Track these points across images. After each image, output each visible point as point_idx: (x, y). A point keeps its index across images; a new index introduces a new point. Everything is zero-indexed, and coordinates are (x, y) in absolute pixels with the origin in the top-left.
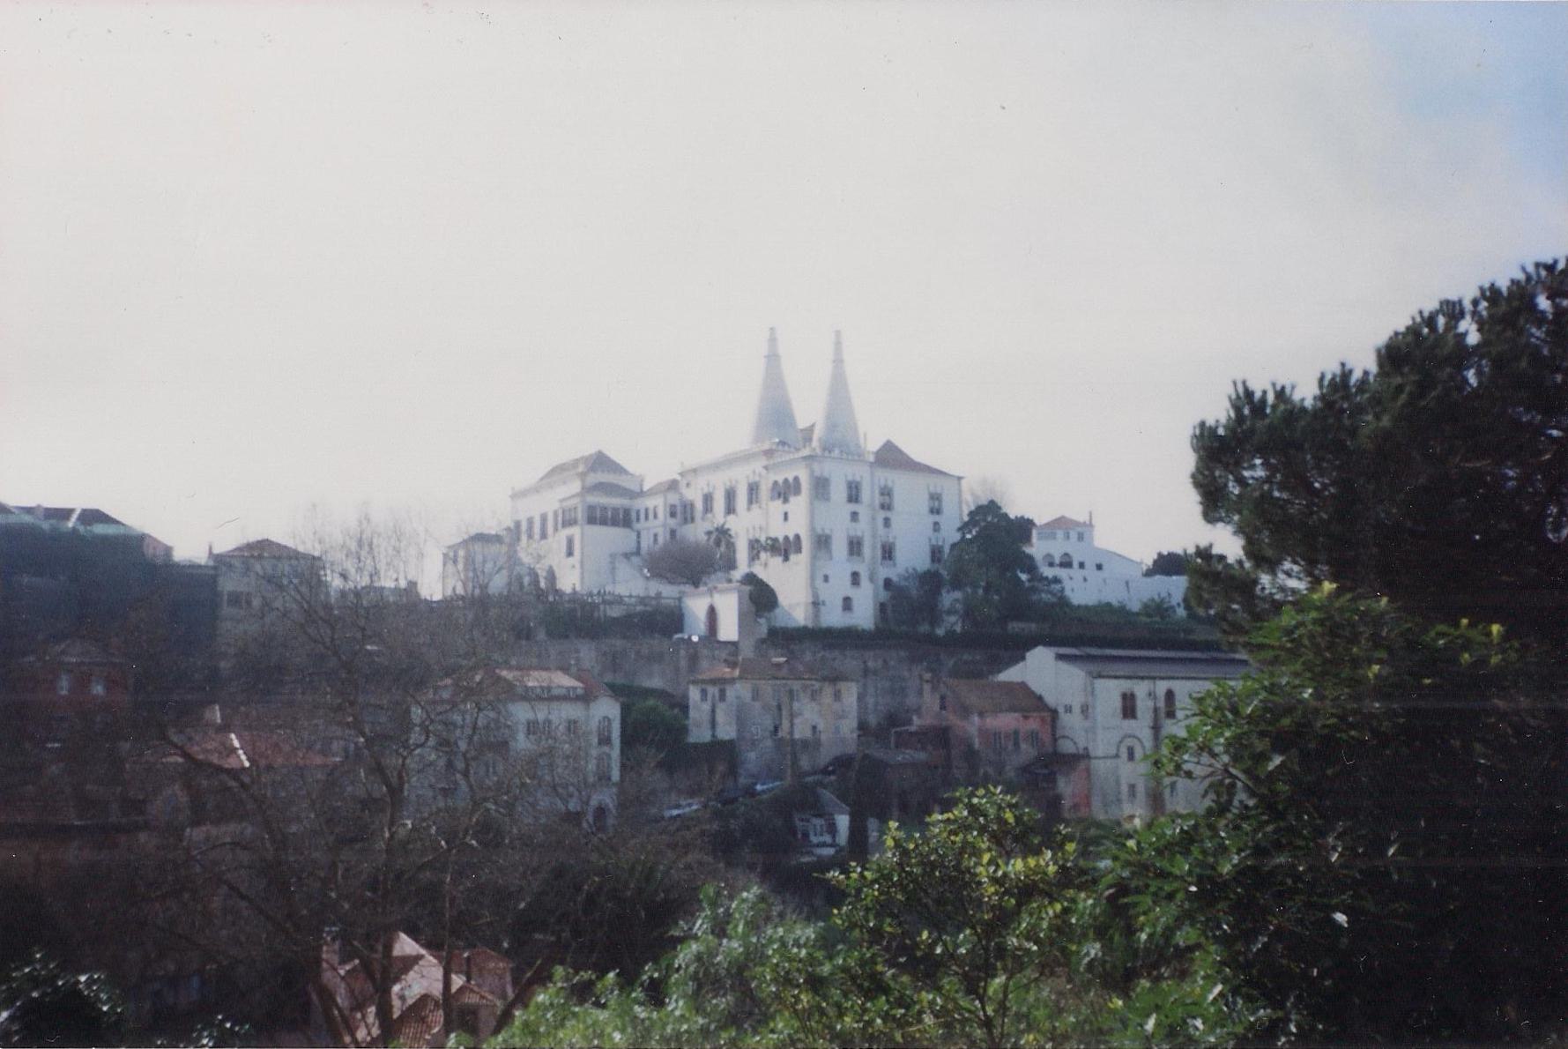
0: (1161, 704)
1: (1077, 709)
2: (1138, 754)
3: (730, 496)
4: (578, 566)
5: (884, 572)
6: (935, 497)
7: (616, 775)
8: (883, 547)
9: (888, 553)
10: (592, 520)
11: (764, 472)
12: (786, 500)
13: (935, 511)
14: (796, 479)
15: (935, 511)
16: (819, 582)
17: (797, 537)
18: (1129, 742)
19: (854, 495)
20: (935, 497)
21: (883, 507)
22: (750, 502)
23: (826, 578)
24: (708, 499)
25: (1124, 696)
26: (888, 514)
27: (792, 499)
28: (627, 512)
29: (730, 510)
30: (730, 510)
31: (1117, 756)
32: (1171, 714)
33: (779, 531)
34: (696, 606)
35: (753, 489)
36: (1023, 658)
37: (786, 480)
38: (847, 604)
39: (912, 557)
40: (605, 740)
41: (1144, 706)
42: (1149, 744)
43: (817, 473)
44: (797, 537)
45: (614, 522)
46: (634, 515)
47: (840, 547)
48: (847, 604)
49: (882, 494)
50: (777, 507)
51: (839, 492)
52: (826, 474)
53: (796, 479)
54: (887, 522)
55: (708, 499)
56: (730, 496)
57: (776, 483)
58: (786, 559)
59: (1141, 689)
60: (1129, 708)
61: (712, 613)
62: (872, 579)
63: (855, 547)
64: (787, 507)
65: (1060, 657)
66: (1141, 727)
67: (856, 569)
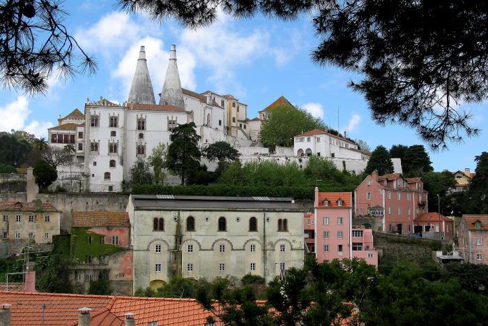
0: (184, 224)
2: (164, 248)
19: (114, 122)
23: (95, 164)
31: (148, 250)
38: (107, 176)
41: (170, 225)
43: (92, 113)
47: (104, 148)
48: (107, 176)
51: (104, 121)
52: (97, 114)
54: (141, 136)
59: (169, 217)
60: (159, 225)
62: (122, 163)
63: (113, 148)
66: (168, 235)
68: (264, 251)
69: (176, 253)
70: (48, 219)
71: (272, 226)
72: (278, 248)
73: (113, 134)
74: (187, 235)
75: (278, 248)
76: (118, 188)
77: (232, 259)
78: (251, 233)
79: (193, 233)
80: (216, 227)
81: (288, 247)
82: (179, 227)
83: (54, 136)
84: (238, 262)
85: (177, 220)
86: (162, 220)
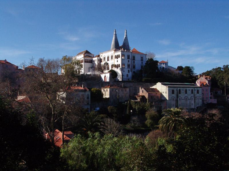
1: (165, 92)
2: (175, 99)
3: (108, 58)
4: (83, 69)
5: (133, 70)
6: (142, 58)
7: (90, 104)
8: (133, 66)
9: (134, 67)
10: (85, 62)
11: (113, 54)
12: (117, 59)
13: (142, 60)
14: (119, 55)
15: (142, 60)
16: (123, 72)
17: (119, 64)
18: (173, 98)
20: (142, 58)
21: (133, 59)
22: (111, 59)
24: (104, 58)
25: (172, 90)
26: (134, 61)
27: (118, 58)
28: (91, 60)
29: (108, 60)
30: (108, 60)
31: (171, 100)
32: (180, 93)
33: (116, 63)
34: (103, 76)
35: (112, 57)
36: (156, 84)
37: (117, 55)
39: (138, 67)
40: (88, 98)
41: (175, 92)
42: (176, 98)
44: (119, 64)
45: (89, 62)
46: (92, 61)
49: (133, 57)
50: (116, 60)
52: (124, 54)
53: (119, 55)
54: (134, 62)
55: (104, 58)
56: (108, 58)
57: (116, 56)
58: (117, 68)
61: (105, 76)
62: (131, 71)
63: (129, 66)
64: (117, 60)
65: (162, 84)
67: (129, 70)
68: (195, 100)
69: (177, 101)
70: (126, 91)
71: (196, 92)
72: (197, 99)
73: (129, 61)
74: (179, 95)
75: (197, 99)
76: (130, 80)
77: (188, 102)
78: (198, 94)
79: (180, 94)
80: (185, 93)
81: (199, 98)
82: (177, 92)
83: (85, 60)
84: (189, 103)
85: (177, 90)
86: (174, 90)
